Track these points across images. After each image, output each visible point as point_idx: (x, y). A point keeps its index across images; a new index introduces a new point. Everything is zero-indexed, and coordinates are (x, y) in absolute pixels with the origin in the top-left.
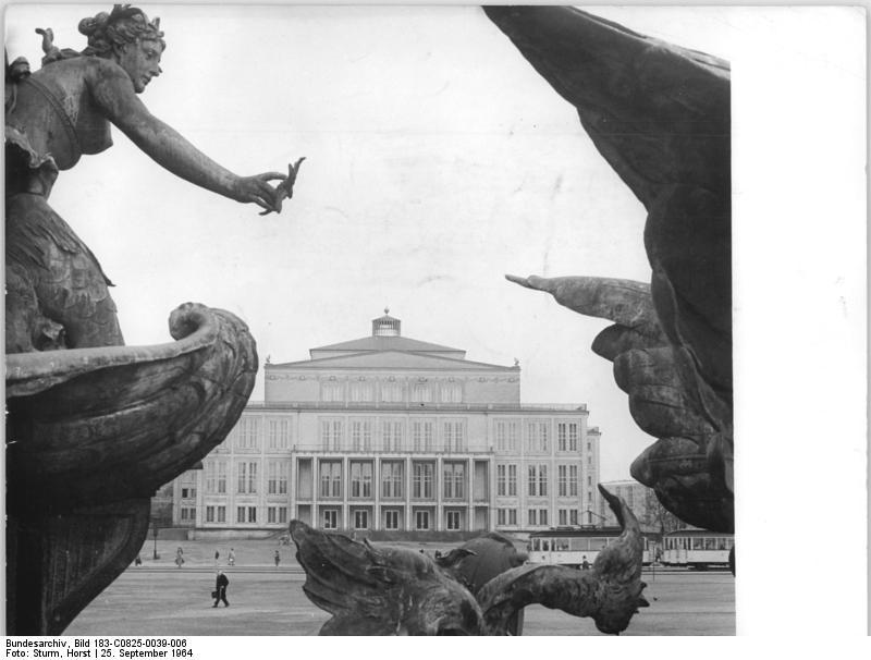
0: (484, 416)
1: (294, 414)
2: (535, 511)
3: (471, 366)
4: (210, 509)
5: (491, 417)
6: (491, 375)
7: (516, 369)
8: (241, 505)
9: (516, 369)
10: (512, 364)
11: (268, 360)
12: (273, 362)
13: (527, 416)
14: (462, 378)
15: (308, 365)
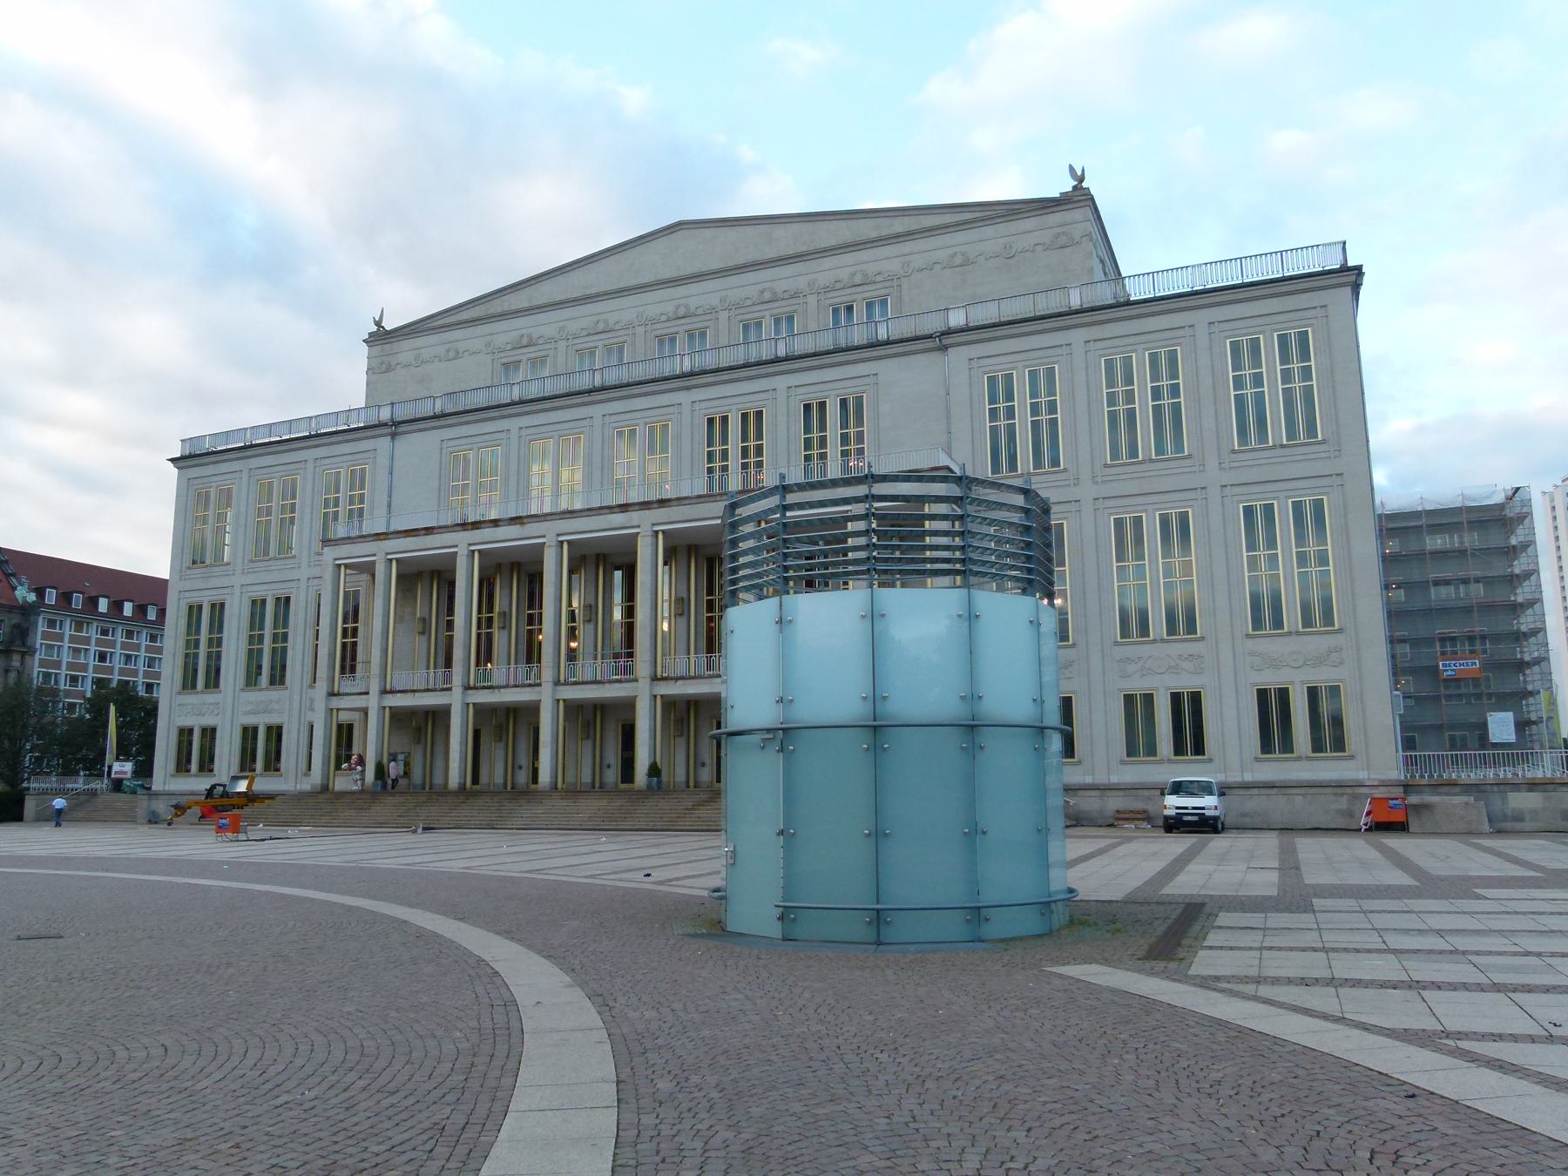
0: (936, 356)
1: (383, 444)
2: (1149, 699)
3: (899, 226)
4: (185, 734)
5: (958, 356)
6: (991, 237)
7: (1079, 198)
8: (250, 720)
9: (1079, 198)
10: (1060, 185)
11: (378, 323)
12: (389, 325)
13: (1096, 332)
14: (894, 266)
15: (465, 315)
